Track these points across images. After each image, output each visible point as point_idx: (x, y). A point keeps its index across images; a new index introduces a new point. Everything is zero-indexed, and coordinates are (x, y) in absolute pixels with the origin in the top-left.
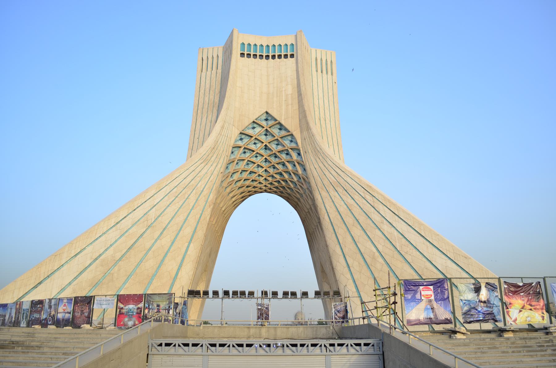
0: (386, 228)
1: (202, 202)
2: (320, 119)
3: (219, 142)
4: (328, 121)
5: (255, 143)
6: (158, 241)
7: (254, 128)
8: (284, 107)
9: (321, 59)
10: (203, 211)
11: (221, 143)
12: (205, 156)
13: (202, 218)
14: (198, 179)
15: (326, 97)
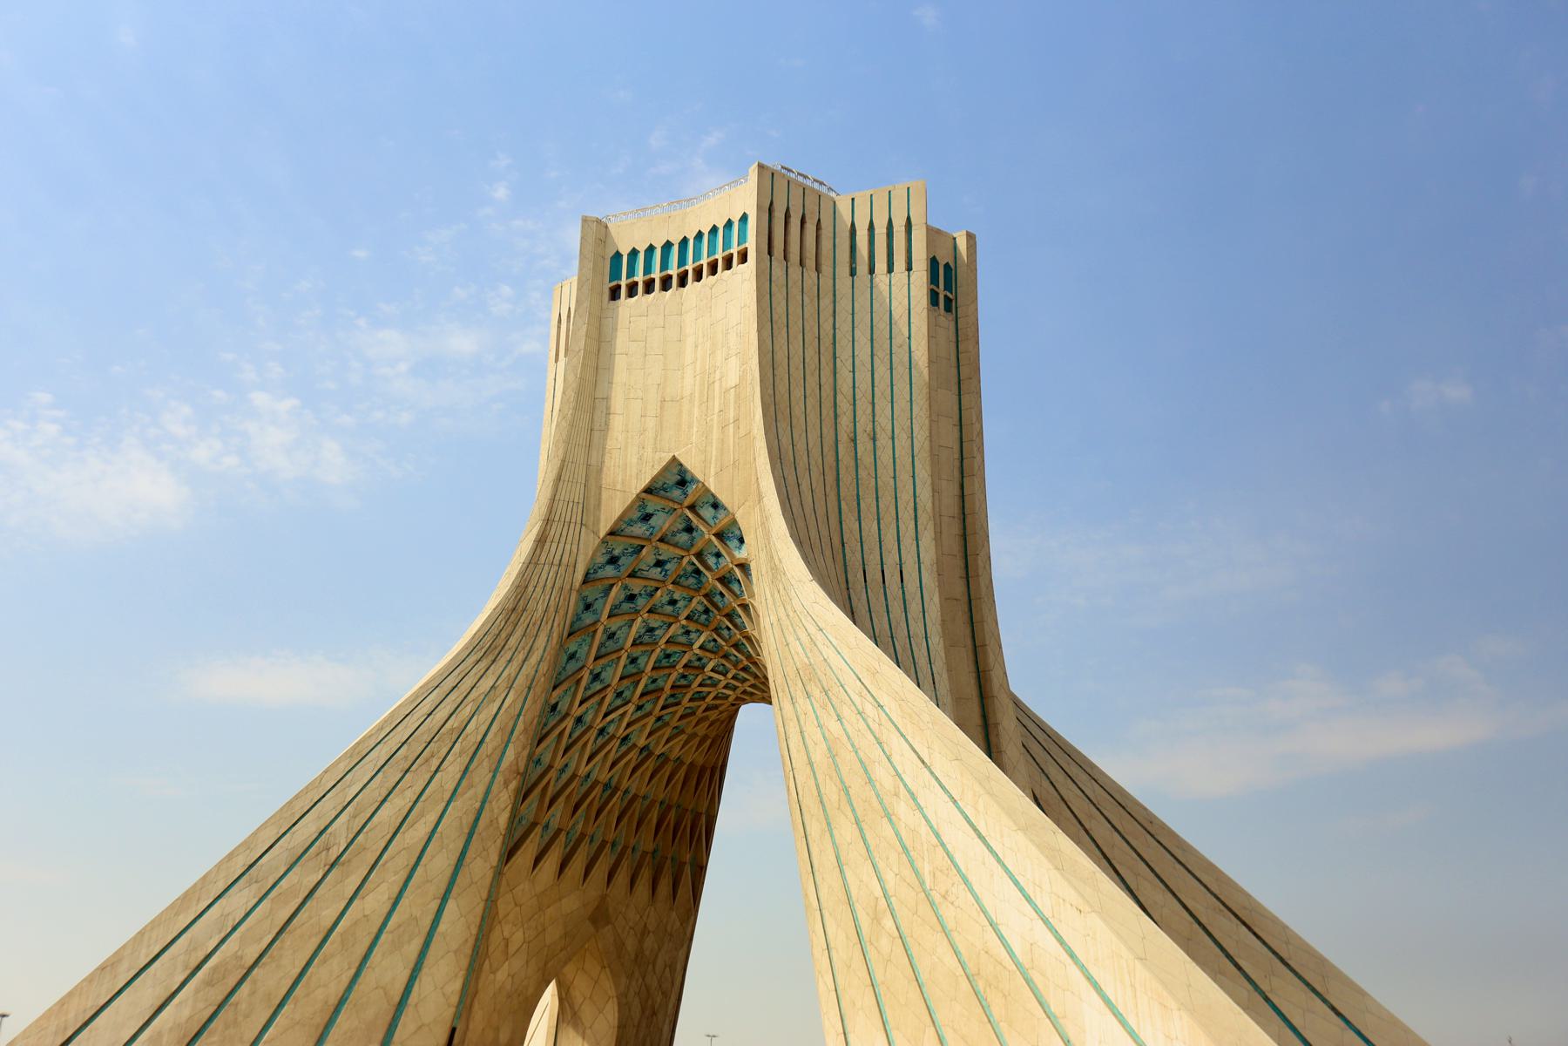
0: (902, 808)
1: (481, 775)
2: (854, 440)
3: (530, 589)
4: (883, 440)
5: (659, 564)
6: (356, 902)
7: (646, 518)
8: (715, 435)
9: (871, 227)
10: (483, 802)
11: (539, 590)
12: (489, 639)
13: (482, 824)
14: (466, 711)
15: (882, 354)
